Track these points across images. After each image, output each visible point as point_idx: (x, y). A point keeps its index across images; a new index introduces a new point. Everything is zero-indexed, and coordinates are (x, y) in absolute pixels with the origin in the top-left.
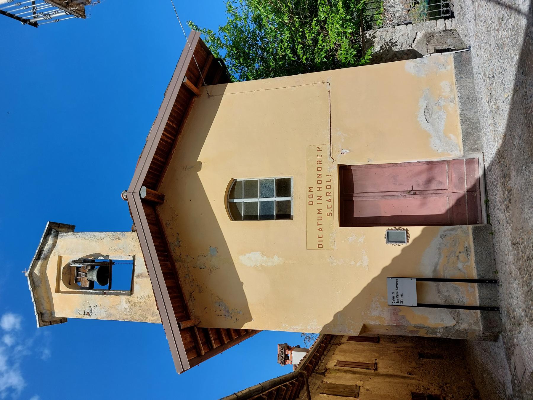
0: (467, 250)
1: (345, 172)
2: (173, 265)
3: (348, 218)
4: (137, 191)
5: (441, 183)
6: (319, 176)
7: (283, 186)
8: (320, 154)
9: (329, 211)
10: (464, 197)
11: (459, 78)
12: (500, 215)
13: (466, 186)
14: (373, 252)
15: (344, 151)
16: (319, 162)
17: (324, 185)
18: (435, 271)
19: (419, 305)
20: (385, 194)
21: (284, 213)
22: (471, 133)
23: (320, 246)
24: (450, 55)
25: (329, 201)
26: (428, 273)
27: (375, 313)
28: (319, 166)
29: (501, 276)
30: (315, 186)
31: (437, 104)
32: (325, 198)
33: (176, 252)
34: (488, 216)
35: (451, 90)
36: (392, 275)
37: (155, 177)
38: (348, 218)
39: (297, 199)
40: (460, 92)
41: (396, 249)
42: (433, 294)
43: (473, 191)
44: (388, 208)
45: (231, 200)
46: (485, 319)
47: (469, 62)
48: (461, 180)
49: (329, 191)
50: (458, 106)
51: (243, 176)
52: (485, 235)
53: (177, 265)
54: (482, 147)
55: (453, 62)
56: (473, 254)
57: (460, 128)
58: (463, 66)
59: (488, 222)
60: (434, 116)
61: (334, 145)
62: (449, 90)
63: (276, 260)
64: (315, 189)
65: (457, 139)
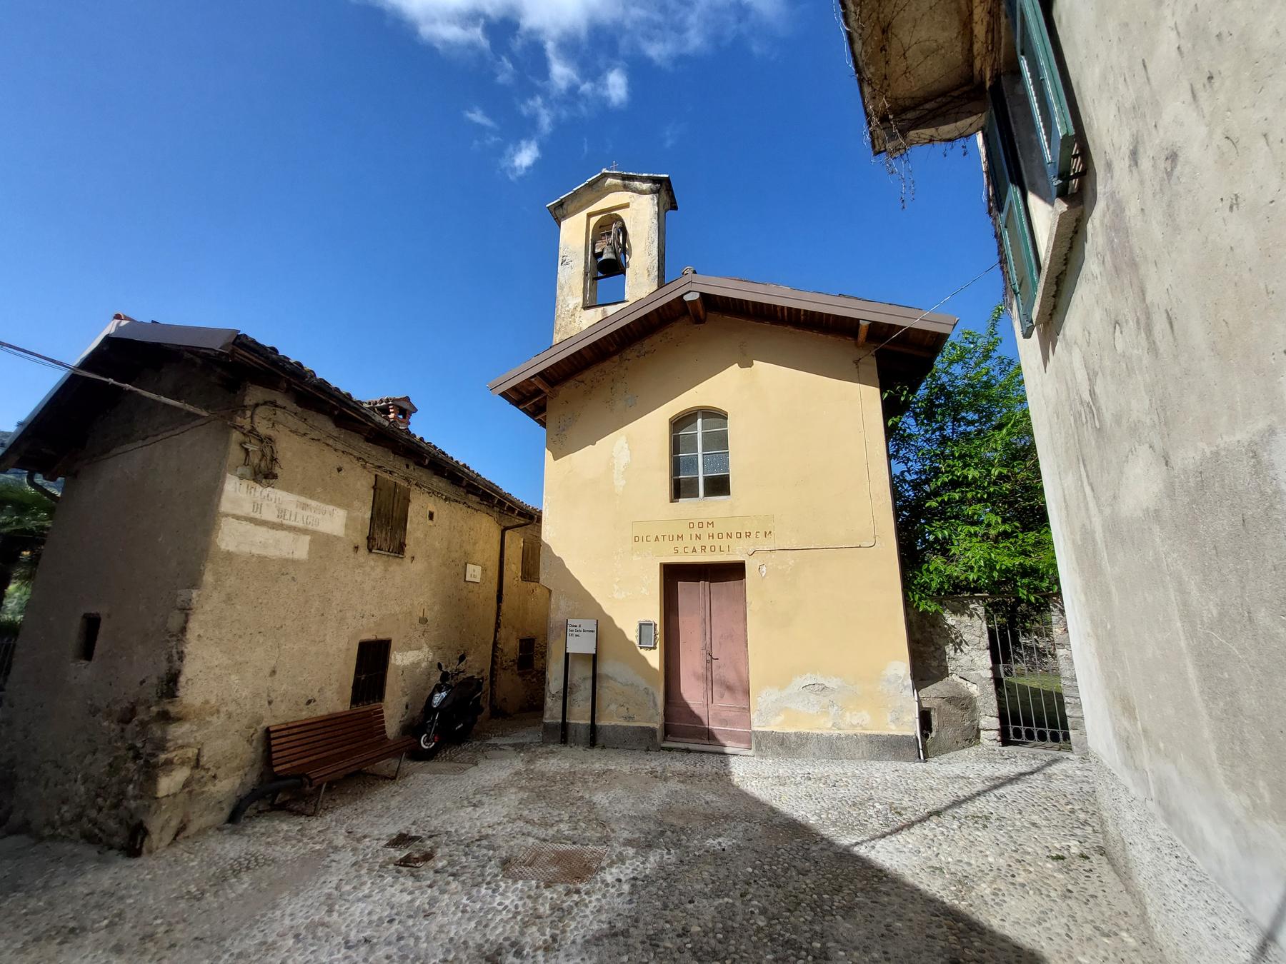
0: (630, 718)
1: (734, 571)
2: (614, 353)
3: (673, 575)
4: (694, 287)
5: (722, 697)
6: (729, 536)
7: (719, 486)
8: (761, 535)
9: (681, 550)
10: (701, 722)
11: (872, 739)
12: (679, 765)
13: (715, 727)
14: (632, 605)
15: (764, 569)
16: (748, 535)
17: (716, 542)
18: (608, 677)
19: (567, 655)
20: (708, 621)
21: (680, 489)
22: (784, 745)
23: (636, 539)
24: (914, 729)
25: (694, 550)
26: (605, 668)
27: (562, 603)
28: (743, 535)
29: (596, 751)
30: (715, 530)
31: (832, 704)
32: (698, 544)
33: (631, 354)
34: (670, 749)
35: (854, 726)
36: (604, 628)
37: (717, 308)
38: (673, 575)
39: (701, 507)
40: (847, 737)
41: (632, 635)
42: (581, 673)
43: (710, 736)
44: (688, 624)
45: (700, 414)
46: (555, 726)
47: (898, 757)
48: (725, 722)
49: (708, 549)
50: (825, 732)
51: (734, 429)
52: (644, 741)
53: (616, 358)
54: (762, 757)
55: (900, 734)
56: (625, 724)
57: (792, 730)
58: (892, 747)
59: (663, 749)
60: (812, 697)
61: (773, 555)
62: (854, 722)
63: (620, 483)
64: (710, 530)
65: (775, 725)
